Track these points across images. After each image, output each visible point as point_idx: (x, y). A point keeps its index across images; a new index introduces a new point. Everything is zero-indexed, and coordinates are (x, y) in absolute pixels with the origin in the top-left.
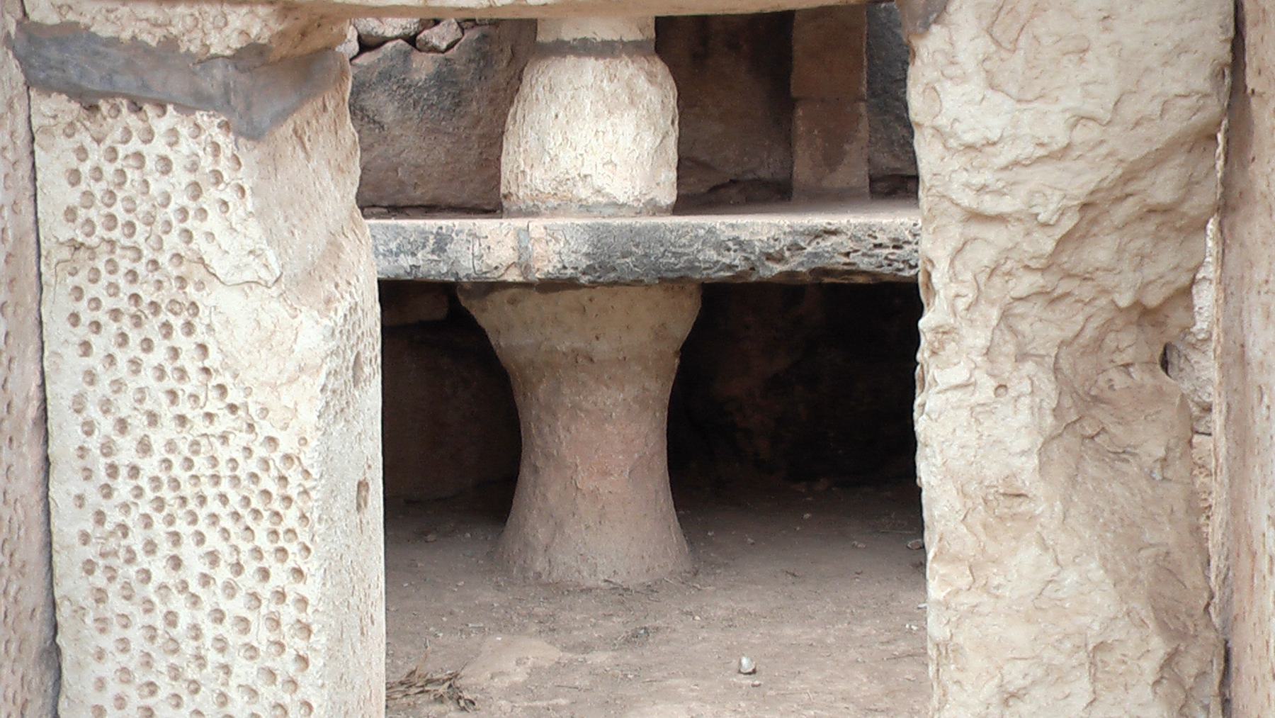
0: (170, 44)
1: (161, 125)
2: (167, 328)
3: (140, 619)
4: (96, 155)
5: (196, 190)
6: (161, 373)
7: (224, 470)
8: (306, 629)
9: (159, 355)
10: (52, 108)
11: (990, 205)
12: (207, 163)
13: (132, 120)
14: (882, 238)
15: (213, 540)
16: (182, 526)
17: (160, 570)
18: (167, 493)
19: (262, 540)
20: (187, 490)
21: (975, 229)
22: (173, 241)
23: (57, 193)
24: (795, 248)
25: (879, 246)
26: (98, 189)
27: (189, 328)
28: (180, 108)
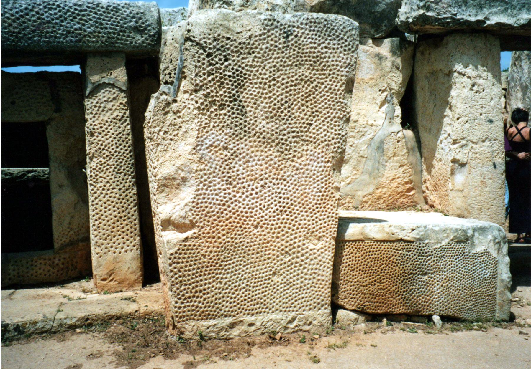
24: (24, 175)
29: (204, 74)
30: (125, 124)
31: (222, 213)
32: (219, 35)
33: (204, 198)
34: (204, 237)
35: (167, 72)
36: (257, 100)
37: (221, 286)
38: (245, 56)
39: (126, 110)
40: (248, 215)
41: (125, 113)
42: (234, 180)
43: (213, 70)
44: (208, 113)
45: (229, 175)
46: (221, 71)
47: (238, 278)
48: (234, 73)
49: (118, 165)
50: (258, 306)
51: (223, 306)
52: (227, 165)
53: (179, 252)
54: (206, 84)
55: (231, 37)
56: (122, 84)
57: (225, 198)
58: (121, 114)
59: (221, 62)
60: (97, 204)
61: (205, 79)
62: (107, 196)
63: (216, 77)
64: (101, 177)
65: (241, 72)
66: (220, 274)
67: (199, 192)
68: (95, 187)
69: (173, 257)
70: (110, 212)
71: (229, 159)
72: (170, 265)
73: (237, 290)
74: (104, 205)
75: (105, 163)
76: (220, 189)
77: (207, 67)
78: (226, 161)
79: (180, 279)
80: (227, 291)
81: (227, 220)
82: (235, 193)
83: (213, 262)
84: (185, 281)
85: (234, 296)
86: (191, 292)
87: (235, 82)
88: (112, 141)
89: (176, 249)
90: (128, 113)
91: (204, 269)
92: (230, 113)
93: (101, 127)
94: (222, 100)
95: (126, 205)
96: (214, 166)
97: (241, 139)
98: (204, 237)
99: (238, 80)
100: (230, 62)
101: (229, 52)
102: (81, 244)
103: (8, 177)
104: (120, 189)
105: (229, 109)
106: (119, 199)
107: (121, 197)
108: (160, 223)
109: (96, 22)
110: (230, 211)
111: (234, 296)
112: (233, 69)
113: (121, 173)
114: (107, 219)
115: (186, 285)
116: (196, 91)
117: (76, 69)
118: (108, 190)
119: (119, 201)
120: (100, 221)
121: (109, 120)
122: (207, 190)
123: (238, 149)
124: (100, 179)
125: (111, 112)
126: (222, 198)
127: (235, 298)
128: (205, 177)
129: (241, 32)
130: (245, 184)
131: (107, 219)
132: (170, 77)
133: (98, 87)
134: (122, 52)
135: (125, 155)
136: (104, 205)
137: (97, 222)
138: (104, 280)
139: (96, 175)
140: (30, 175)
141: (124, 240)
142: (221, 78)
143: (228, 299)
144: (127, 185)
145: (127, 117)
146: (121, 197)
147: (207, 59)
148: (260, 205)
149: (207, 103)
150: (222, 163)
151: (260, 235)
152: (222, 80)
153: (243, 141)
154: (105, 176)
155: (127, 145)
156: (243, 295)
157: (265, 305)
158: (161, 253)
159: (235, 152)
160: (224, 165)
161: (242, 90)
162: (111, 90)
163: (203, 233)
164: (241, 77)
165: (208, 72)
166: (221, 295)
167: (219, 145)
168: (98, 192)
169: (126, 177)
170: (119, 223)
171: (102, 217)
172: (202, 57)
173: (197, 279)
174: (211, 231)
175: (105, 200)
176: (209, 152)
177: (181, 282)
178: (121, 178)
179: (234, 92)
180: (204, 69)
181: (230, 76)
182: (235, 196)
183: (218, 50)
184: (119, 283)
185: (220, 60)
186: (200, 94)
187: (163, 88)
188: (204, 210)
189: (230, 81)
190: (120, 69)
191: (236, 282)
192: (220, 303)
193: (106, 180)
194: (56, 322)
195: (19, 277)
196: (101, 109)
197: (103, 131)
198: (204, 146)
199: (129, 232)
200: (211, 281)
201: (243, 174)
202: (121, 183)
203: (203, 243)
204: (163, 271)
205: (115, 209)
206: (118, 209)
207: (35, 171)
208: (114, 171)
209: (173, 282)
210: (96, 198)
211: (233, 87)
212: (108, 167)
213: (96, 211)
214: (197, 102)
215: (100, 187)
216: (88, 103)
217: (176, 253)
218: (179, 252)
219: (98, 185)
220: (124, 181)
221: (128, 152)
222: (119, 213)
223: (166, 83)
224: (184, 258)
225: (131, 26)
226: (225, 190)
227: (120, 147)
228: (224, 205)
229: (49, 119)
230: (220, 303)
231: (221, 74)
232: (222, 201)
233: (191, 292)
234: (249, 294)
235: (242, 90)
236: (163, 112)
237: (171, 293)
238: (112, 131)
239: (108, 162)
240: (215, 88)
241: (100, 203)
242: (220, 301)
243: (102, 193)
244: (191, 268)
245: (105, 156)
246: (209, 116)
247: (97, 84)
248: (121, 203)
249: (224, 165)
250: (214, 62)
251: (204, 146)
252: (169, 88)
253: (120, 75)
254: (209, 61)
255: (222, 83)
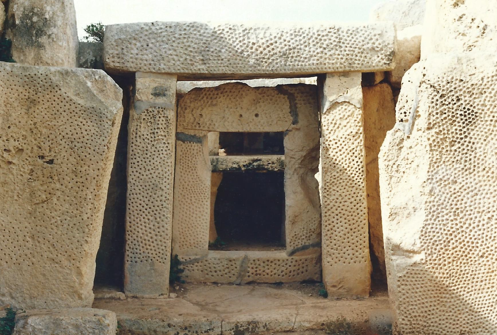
0: (195, 135)
1: (193, 145)
2: (192, 170)
3: (186, 207)
4: (185, 148)
5: (197, 153)
6: (191, 175)
7: (198, 188)
8: (207, 209)
9: (191, 173)
10: (179, 142)
11: (293, 156)
12: (199, 149)
13: (190, 144)
14: (270, 162)
15: (196, 197)
16: (192, 195)
17: (189, 201)
18: (191, 191)
19: (202, 197)
20: (193, 190)
21: (292, 159)
22: (194, 159)
23: (179, 153)
24: (250, 164)
25: (269, 164)
26: (185, 153)
27: (195, 170)
28: (196, 143)
29: (437, 114)
30: (359, 141)
31: (449, 242)
32: (453, 78)
33: (432, 228)
34: (431, 264)
35: (402, 111)
36: (487, 137)
37: (445, 309)
38: (477, 96)
39: (360, 126)
40: (474, 245)
41: (359, 130)
42: (462, 212)
43: (445, 110)
44: (440, 150)
45: (457, 207)
46: (453, 110)
47: (461, 302)
48: (465, 112)
49: (350, 180)
50: (480, 330)
51: (446, 327)
52: (456, 198)
53: (407, 275)
54: (439, 123)
55: (464, 79)
56: (357, 101)
57: (452, 228)
58: (355, 131)
59: (454, 102)
60: (330, 215)
61: (437, 118)
62: (339, 209)
63: (449, 116)
64: (334, 190)
65: (473, 111)
66: (445, 297)
67: (427, 223)
68: (328, 199)
69: (401, 279)
70: (341, 224)
71: (458, 192)
72: (399, 287)
73: (460, 314)
74: (336, 217)
75: (338, 177)
76: (447, 220)
77: (441, 107)
78: (455, 193)
79: (407, 300)
80: (451, 314)
81: (453, 248)
82: (462, 224)
83: (438, 287)
84: (412, 302)
85: (457, 319)
86: (417, 312)
87: (466, 120)
88: (346, 157)
89: (405, 272)
90: (362, 129)
91: (429, 293)
92: (460, 150)
93: (336, 143)
94: (453, 137)
95: (356, 218)
96: (443, 198)
97: (470, 173)
98: (431, 264)
99: (470, 118)
100: (461, 102)
101: (462, 93)
102: (311, 248)
103: (235, 166)
104: (351, 203)
105: (460, 145)
106: (350, 212)
107: (352, 210)
108: (391, 248)
109: (336, 45)
110: (457, 241)
111: (457, 319)
112: (464, 108)
113: (353, 187)
114: (338, 230)
115: (412, 305)
116: (429, 129)
117: (312, 81)
118: (340, 203)
119: (350, 214)
120: (331, 231)
121: (344, 137)
122: (435, 220)
123: (467, 183)
124: (333, 192)
125: (345, 129)
126: (449, 228)
127: (458, 320)
128: (434, 209)
129: (474, 74)
130: (473, 216)
131: (338, 230)
132: (405, 116)
133: (335, 105)
134: (358, 71)
135: (357, 170)
136: (336, 217)
137: (329, 233)
138: (334, 286)
139: (330, 188)
140: (255, 164)
141: (353, 251)
142: (453, 116)
143: (451, 321)
144: (358, 199)
145: (361, 133)
146: (352, 210)
147: (440, 100)
148: (487, 236)
149: (439, 140)
150: (451, 196)
151: (485, 265)
152: (454, 119)
153: (472, 175)
154: (338, 189)
155: (359, 161)
156: (466, 319)
157: (487, 329)
158: (390, 274)
159: (463, 186)
160: (452, 198)
161: (473, 127)
162: (346, 107)
163: (430, 260)
164: (473, 115)
165: (441, 111)
166: (445, 317)
167: (449, 179)
168: (331, 204)
169: (358, 191)
170: (349, 235)
171: (334, 228)
172: (435, 98)
173: (423, 301)
174: (437, 259)
175: (337, 212)
176: (438, 186)
177: (408, 302)
178: (353, 192)
179: (465, 130)
180: (437, 109)
181: (461, 115)
182: (462, 227)
183: (451, 91)
184: (347, 292)
185: (453, 100)
186: (434, 131)
187: (398, 125)
188: (431, 239)
189: (462, 119)
190: (355, 88)
191: (460, 306)
192: (443, 324)
193: (339, 193)
194: (296, 324)
195: (256, 275)
196: (336, 126)
197: (338, 147)
198: (434, 181)
199: (358, 244)
200: (436, 303)
201: (470, 206)
202: (353, 197)
203: (429, 268)
204: (392, 290)
205: (346, 221)
206: (349, 221)
207: (260, 160)
208: (346, 185)
209: (401, 302)
210: (329, 210)
211: (465, 125)
212: (341, 181)
213: (328, 222)
214: (429, 139)
215: (333, 200)
216: (325, 120)
217: (405, 276)
218: (407, 275)
219: (331, 198)
220: (355, 195)
221: (360, 167)
222: (350, 225)
223: (402, 120)
224: (412, 281)
225: (368, 48)
226: (452, 221)
227: (353, 162)
228: (451, 235)
229: (287, 130)
230: (443, 324)
231: (453, 113)
232: (449, 231)
233: (417, 312)
234: (472, 318)
235: (473, 127)
236: (397, 148)
237: (398, 311)
238: (345, 147)
239: (341, 177)
240: (447, 127)
241: (333, 215)
242: (443, 322)
243: (334, 206)
244: (418, 290)
245: (338, 170)
246: (440, 152)
247: (334, 102)
248: (352, 216)
249: (452, 198)
250: (447, 103)
251: (434, 181)
252: (404, 126)
253: (356, 93)
254: (442, 102)
255: (455, 121)
